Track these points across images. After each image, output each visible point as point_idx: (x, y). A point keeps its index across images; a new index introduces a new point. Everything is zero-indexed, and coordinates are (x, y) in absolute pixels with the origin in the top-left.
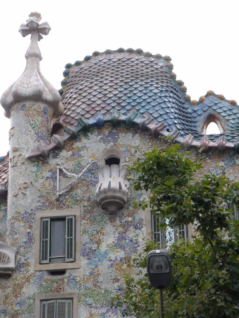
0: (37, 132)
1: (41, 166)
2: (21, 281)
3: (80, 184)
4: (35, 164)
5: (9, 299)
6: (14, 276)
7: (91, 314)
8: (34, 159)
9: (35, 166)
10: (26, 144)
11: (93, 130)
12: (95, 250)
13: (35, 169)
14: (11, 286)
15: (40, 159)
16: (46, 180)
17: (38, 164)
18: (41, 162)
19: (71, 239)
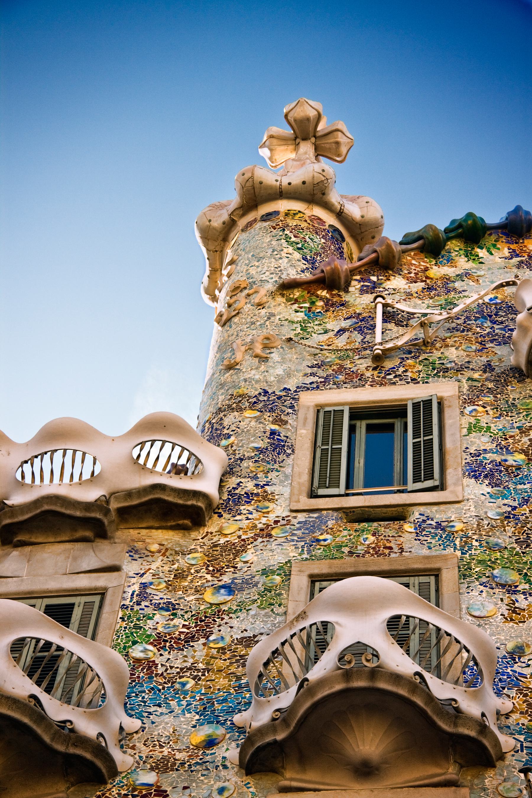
0: (309, 258)
1: (320, 312)
2: (239, 537)
3: (456, 339)
4: (301, 308)
5: (190, 578)
6: (213, 525)
7: (516, 608)
8: (297, 293)
9: (302, 312)
10: (272, 274)
11: (494, 246)
12: (519, 468)
13: (301, 316)
14: (200, 550)
15: (317, 296)
16: (336, 335)
17: (309, 308)
18: (320, 303)
19: (429, 444)
